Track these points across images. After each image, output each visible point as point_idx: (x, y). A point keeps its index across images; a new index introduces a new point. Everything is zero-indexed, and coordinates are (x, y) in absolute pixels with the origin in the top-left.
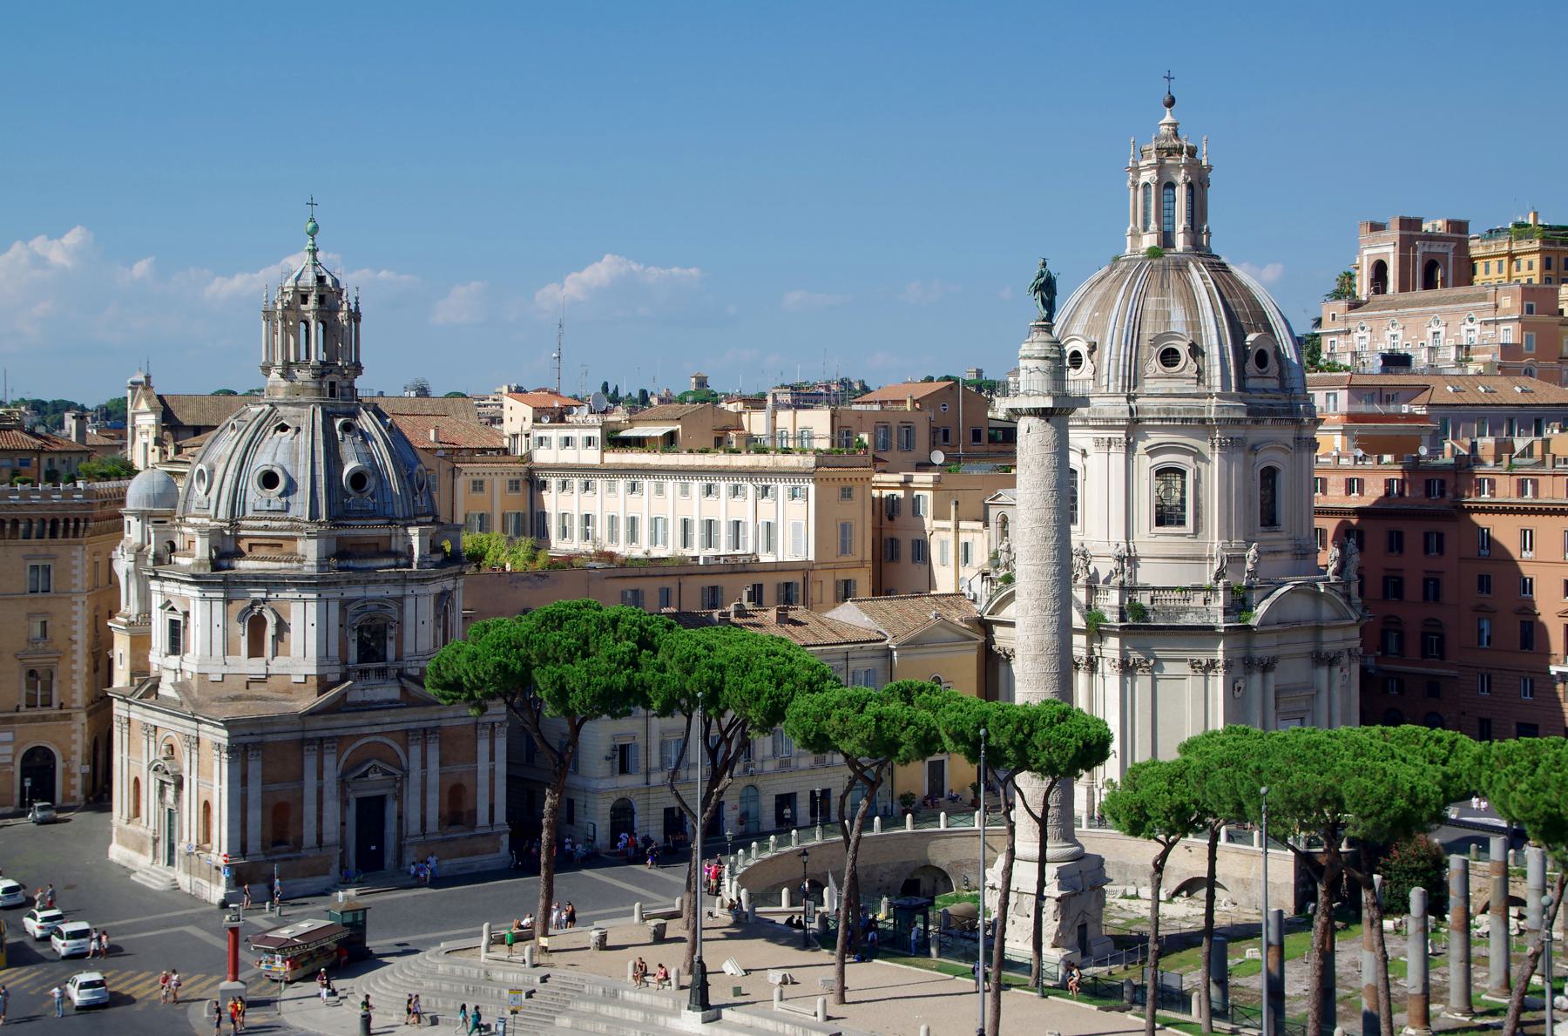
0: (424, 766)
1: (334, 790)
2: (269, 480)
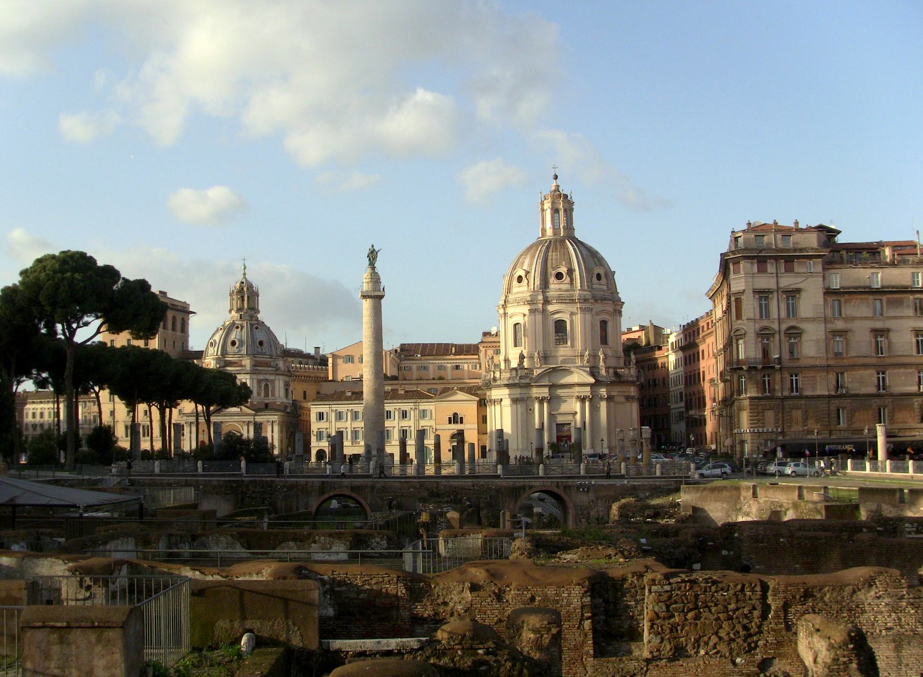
2: (233, 343)
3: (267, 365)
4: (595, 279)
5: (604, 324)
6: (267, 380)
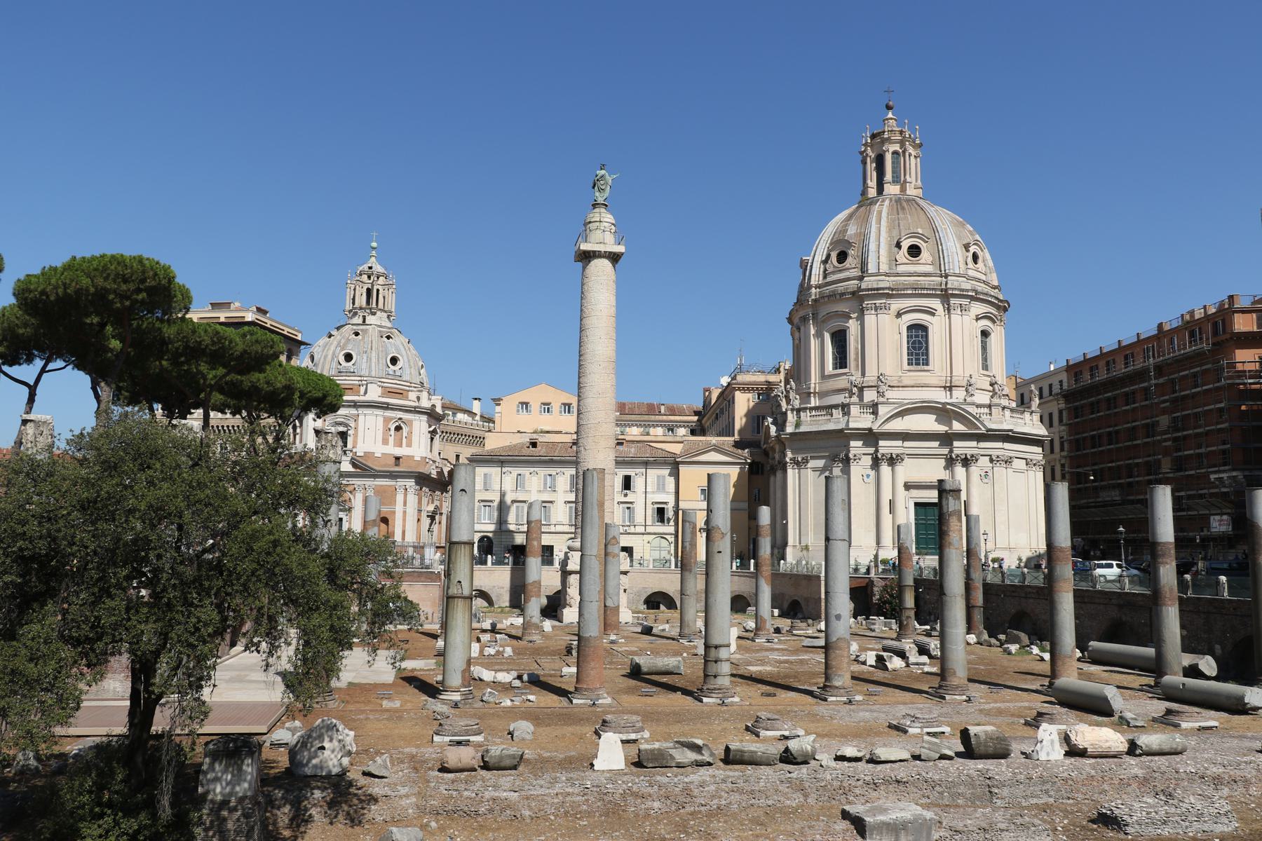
3: (399, 394)
4: (970, 259)
5: (985, 334)
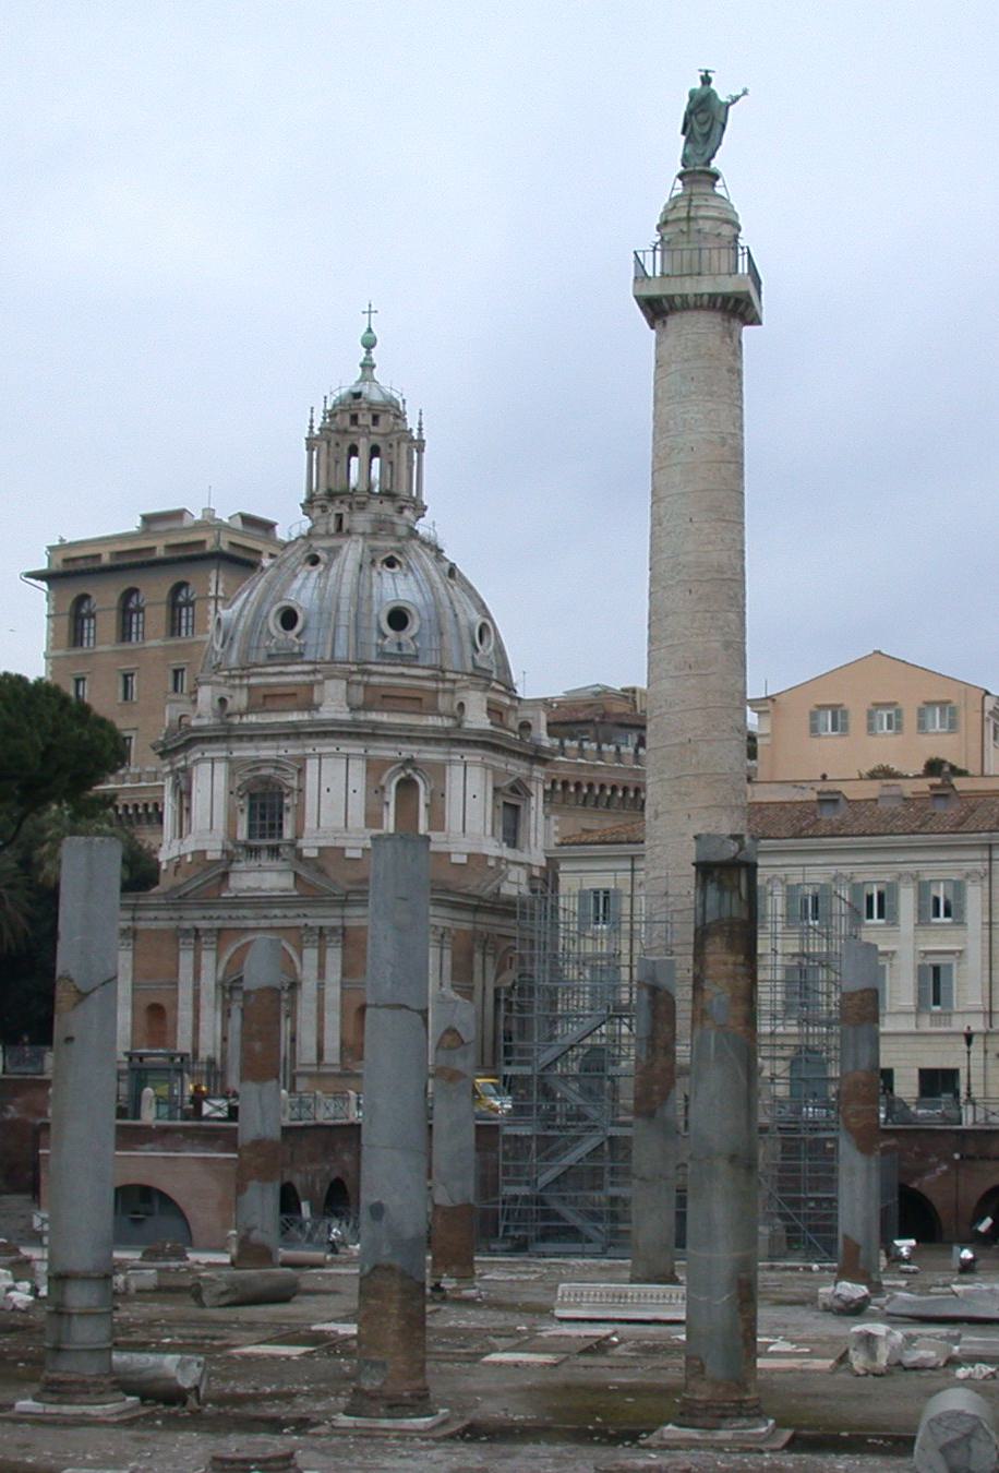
0: (321, 975)
1: (212, 996)
3: (416, 701)
6: (409, 762)
